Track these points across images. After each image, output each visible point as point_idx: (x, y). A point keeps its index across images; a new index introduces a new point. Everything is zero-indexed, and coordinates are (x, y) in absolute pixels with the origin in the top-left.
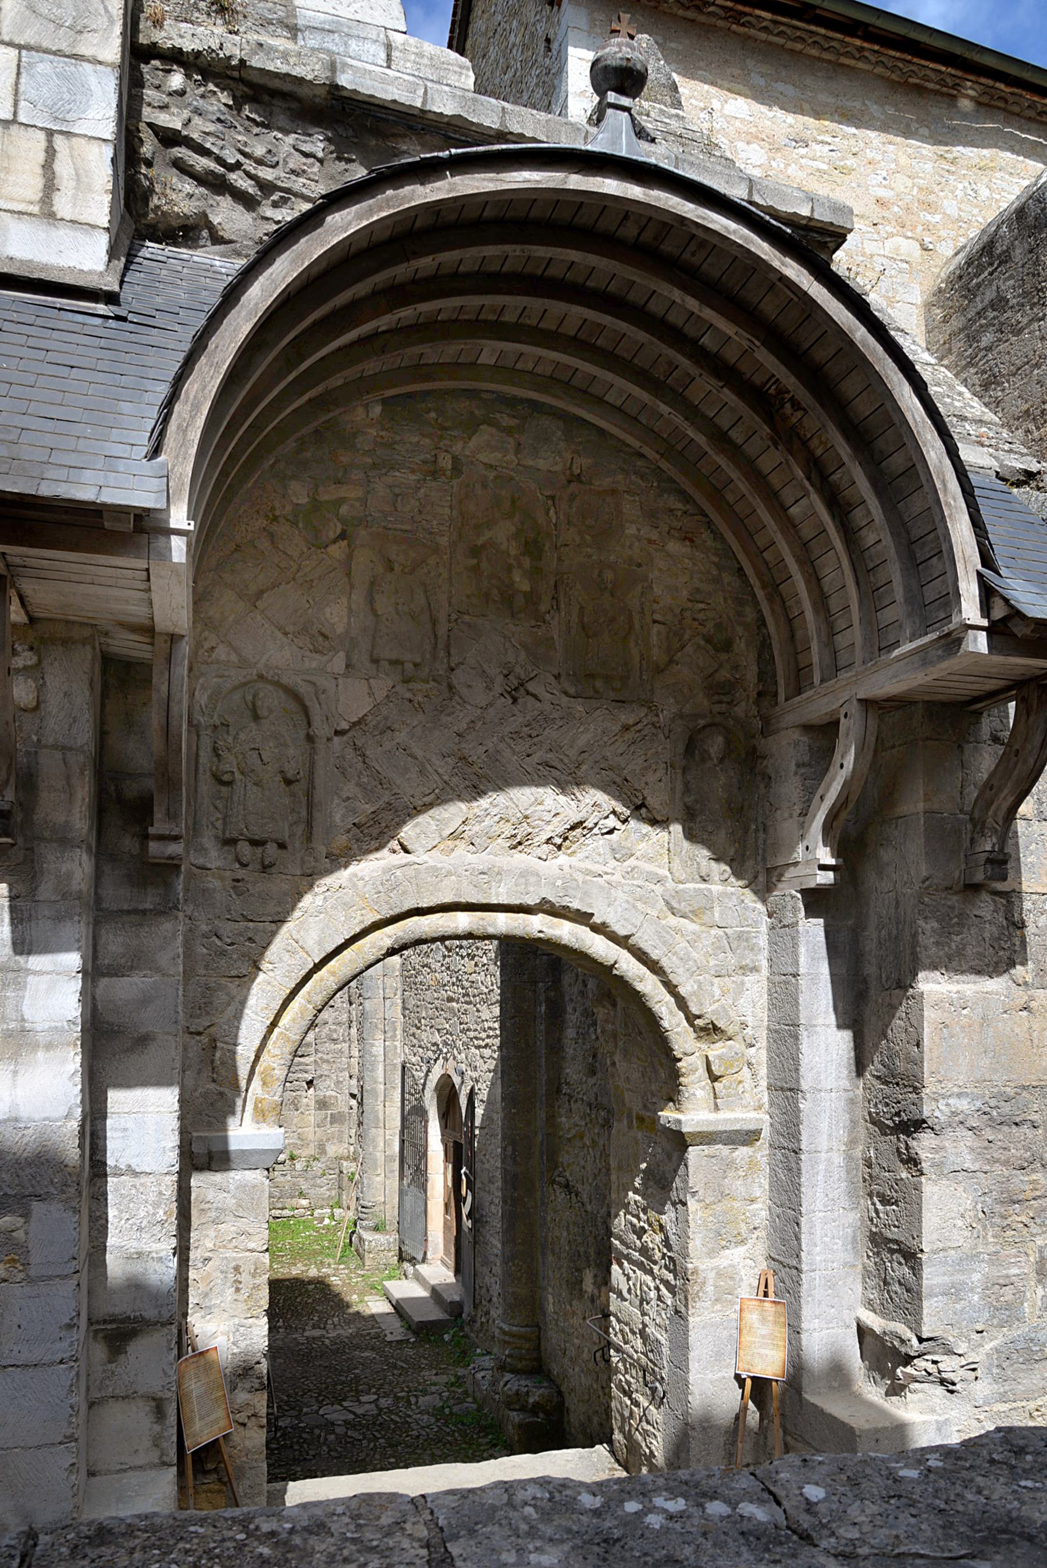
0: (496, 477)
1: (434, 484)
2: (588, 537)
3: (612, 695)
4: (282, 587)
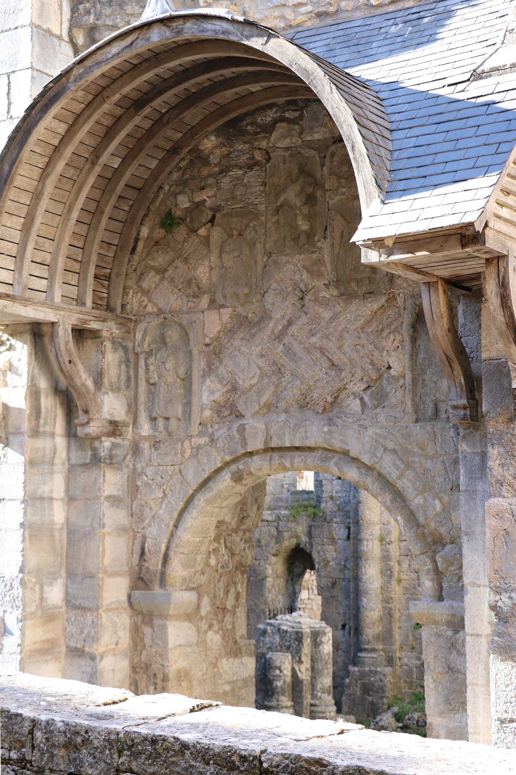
0: (290, 155)
1: (251, 173)
2: (343, 181)
3: (364, 289)
4: (176, 262)
